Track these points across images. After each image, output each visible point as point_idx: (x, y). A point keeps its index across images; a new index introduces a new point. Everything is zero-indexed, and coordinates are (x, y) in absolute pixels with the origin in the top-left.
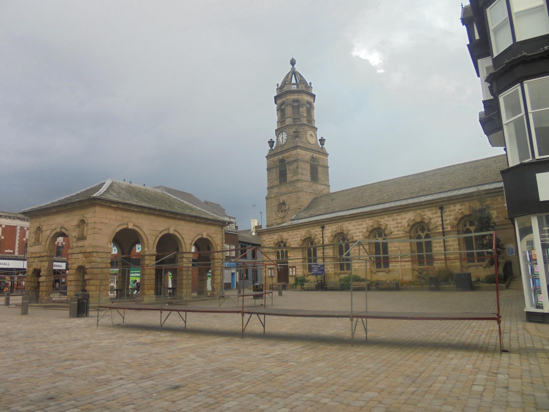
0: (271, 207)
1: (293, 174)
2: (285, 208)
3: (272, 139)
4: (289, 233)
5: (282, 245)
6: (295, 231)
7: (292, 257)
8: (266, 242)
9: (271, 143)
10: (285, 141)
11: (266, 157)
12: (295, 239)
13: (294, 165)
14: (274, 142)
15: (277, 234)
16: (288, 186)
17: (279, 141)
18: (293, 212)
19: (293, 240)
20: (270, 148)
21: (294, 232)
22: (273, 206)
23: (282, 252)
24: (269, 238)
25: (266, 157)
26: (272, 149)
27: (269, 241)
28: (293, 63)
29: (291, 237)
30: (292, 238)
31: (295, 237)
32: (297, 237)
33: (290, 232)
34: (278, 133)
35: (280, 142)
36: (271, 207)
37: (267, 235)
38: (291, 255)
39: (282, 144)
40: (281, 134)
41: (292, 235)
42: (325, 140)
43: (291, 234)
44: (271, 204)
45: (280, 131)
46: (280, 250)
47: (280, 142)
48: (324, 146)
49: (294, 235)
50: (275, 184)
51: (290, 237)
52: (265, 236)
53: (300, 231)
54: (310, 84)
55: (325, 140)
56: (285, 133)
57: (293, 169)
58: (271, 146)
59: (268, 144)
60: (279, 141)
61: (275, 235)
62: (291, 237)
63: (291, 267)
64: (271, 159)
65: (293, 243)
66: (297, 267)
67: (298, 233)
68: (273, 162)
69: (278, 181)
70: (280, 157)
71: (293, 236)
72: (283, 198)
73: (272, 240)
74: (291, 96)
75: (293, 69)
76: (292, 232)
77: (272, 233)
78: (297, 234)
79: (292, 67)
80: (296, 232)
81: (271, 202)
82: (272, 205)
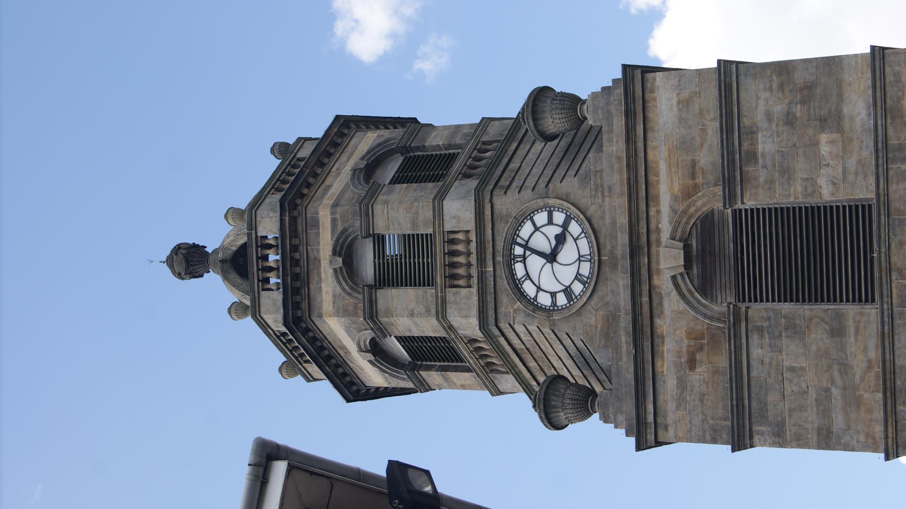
1: (823, 123)
11: (639, 448)
13: (760, 117)
17: (562, 300)
25: (639, 448)
34: (509, 306)
35: (568, 291)
39: (585, 269)
45: (502, 272)
47: (568, 291)
50: (874, 354)
56: (526, 230)
57: (790, 121)
64: (671, 412)
68: (692, 363)
69: (851, 310)
74: (330, 187)
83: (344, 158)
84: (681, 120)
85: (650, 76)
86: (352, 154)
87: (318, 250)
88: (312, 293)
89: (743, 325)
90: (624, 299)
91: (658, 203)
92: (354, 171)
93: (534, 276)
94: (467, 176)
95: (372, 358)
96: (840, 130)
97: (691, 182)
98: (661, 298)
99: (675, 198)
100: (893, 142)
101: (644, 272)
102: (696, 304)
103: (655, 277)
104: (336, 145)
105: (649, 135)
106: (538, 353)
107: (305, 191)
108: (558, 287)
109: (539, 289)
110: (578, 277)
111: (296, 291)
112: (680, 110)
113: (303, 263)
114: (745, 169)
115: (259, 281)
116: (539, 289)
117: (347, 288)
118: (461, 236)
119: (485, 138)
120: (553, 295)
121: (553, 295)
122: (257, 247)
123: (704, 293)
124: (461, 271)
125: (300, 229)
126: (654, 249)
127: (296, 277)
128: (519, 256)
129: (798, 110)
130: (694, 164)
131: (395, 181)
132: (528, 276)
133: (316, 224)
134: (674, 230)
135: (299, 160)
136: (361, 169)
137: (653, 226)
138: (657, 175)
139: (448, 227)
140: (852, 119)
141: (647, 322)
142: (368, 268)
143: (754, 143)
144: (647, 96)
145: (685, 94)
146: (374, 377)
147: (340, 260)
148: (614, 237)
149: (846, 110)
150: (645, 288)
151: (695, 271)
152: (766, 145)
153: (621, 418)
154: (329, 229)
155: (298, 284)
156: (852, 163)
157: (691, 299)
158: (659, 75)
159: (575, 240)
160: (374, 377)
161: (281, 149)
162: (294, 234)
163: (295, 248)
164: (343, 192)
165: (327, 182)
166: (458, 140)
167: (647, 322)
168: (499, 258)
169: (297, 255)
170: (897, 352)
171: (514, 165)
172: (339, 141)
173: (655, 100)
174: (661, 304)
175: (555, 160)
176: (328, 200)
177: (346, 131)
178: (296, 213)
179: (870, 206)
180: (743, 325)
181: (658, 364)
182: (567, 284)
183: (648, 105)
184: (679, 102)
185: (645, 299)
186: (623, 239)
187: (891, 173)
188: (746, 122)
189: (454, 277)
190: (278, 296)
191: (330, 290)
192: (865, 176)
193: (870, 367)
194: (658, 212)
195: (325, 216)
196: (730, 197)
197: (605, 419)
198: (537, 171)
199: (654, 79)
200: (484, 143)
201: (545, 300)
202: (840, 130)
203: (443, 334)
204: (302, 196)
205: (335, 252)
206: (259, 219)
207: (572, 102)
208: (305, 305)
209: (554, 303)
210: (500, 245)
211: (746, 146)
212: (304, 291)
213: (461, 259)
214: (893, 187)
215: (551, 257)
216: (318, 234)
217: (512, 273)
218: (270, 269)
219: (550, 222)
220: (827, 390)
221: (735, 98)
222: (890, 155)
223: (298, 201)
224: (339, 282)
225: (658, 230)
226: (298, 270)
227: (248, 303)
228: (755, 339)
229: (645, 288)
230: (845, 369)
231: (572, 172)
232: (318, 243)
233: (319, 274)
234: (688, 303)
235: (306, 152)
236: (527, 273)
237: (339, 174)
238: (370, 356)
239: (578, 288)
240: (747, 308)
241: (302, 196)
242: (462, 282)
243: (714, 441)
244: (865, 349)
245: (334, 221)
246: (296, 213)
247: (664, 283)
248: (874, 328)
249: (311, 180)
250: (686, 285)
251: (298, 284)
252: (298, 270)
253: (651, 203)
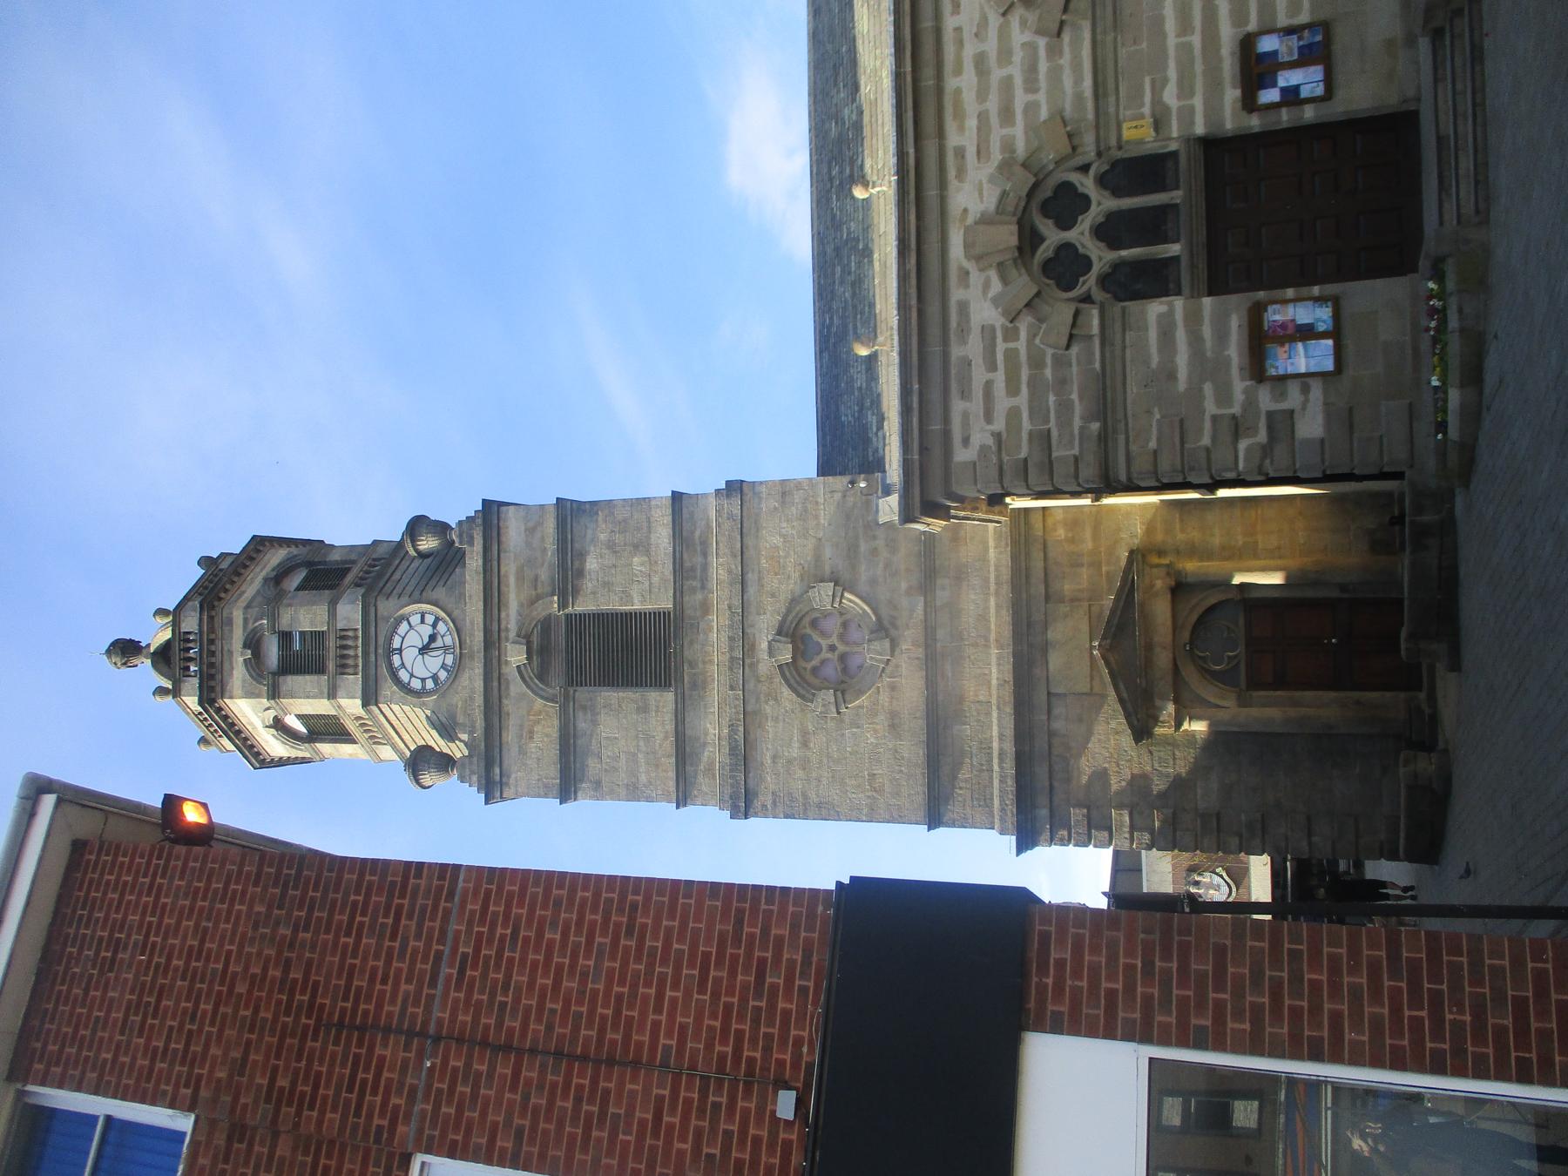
0: (805, 764)
2: (834, 640)
4: (960, 153)
5: (1053, 236)
6: (951, 83)
7: (1157, 89)
8: (1014, 414)
12: (1018, 81)
15: (956, 294)
16: (699, 596)
17: (430, 684)
18: (863, 547)
19: (1020, 99)
21: (958, 91)
22: (805, 744)
23: (1108, 232)
24: (988, 386)
27: (1013, 390)
29: (994, 120)
30: (1007, 115)
31: (997, 74)
32: (1005, 55)
33: (953, 139)
35: (435, 678)
36: (805, 764)
37: (958, 406)
38: (1147, 110)
40: (396, 660)
41: (983, 118)
43: (972, 123)
44: (790, 762)
46: (1101, 257)
47: (435, 678)
49: (982, 95)
50: (670, 727)
51: (997, 135)
52: (966, 441)
53: (958, 30)
57: (611, 546)
58: (445, 763)
61: (964, 307)
62: (994, 120)
63: (1249, 103)
65: (1041, 97)
66: (1252, 26)
67: (969, 51)
69: (653, 696)
70: (515, 656)
71: (993, 105)
72: (764, 627)
73: (1001, 347)
74: (244, 592)
76: (959, 115)
77: (945, 342)
78: (980, 61)
80: (962, 83)
81: (775, 758)
82: (795, 751)
83: (257, 570)
84: (528, 544)
85: (503, 509)
86: (265, 567)
87: (231, 644)
88: (225, 680)
89: (571, 704)
90: (479, 684)
91: (507, 607)
92: (266, 580)
93: (409, 666)
94: (358, 585)
95: (275, 733)
96: (647, 553)
97: (534, 593)
98: (508, 683)
99: (521, 605)
100: (687, 564)
101: (495, 662)
102: (534, 686)
103: (503, 667)
104: (252, 559)
105: (502, 555)
106: (410, 727)
107: (223, 595)
109: (412, 675)
110: (444, 666)
111: (212, 677)
112: (526, 536)
113: (218, 654)
114: (575, 582)
115: (180, 669)
116: (412, 675)
117: (254, 674)
118: (350, 634)
119: (374, 556)
120: (423, 680)
121: (423, 680)
122: (180, 640)
123: (541, 678)
124: (350, 662)
125: (216, 626)
126: (503, 645)
127: (212, 665)
128: (397, 649)
129: (618, 538)
130: (536, 579)
131: (298, 589)
133: (230, 622)
134: (520, 630)
135: (221, 570)
136: (272, 579)
137: (503, 626)
138: (508, 586)
139: (340, 626)
140: (657, 546)
141: (496, 701)
143: (583, 562)
144: (501, 524)
145: (531, 524)
146: (274, 746)
147: (249, 651)
148: (472, 635)
149: (653, 541)
150: (496, 675)
151: (535, 663)
152: (592, 564)
153: (475, 778)
154: (241, 626)
155: (213, 671)
156: (656, 579)
157: (531, 684)
158: (512, 508)
159: (442, 637)
160: (274, 746)
161: (205, 562)
162: (212, 630)
163: (211, 642)
164: (254, 598)
165: (243, 588)
166: (353, 557)
167: (496, 701)
168: (380, 651)
169: (213, 648)
170: (686, 726)
171: (397, 576)
172: (255, 556)
173: (507, 528)
174: (508, 688)
175: (429, 574)
176: (242, 603)
177: (261, 548)
178: (213, 613)
179: (669, 613)
180: (571, 704)
181: (504, 735)
183: (502, 531)
184: (526, 530)
185: (495, 684)
186: (479, 636)
187: (685, 587)
188: (577, 546)
189: (344, 666)
190: (195, 681)
191: (241, 676)
192: (666, 590)
193: (666, 738)
194: (508, 615)
195: (238, 616)
196: (563, 605)
197: (462, 779)
198: (413, 582)
199: (508, 511)
200: (374, 560)
201: (416, 684)
202: (647, 553)
203: (333, 712)
204: (220, 599)
205: (246, 646)
206: (182, 618)
207: (441, 528)
208: (218, 689)
209: (424, 687)
210: (381, 640)
211: (577, 564)
212: (218, 677)
213: (351, 652)
214: (686, 599)
216: (231, 631)
217: (390, 664)
218: (191, 659)
219: (423, 621)
220: (634, 755)
221: (569, 526)
222: (685, 574)
223: (216, 603)
224: (248, 670)
225: (507, 630)
226: (213, 660)
227: (171, 687)
228: (580, 715)
229: (496, 675)
230: (648, 738)
231: (442, 583)
232: (232, 638)
233: (231, 663)
234: (528, 686)
235: (224, 565)
236: (403, 664)
237: (252, 583)
238: (273, 731)
239: (443, 675)
240: (575, 691)
241: (220, 599)
242: (350, 670)
243: (546, 796)
244: (663, 724)
245: (246, 620)
246: (213, 613)
247: (510, 671)
248: (671, 706)
249: (228, 586)
250: (528, 673)
251: (213, 671)
252: (213, 660)
253: (502, 609)
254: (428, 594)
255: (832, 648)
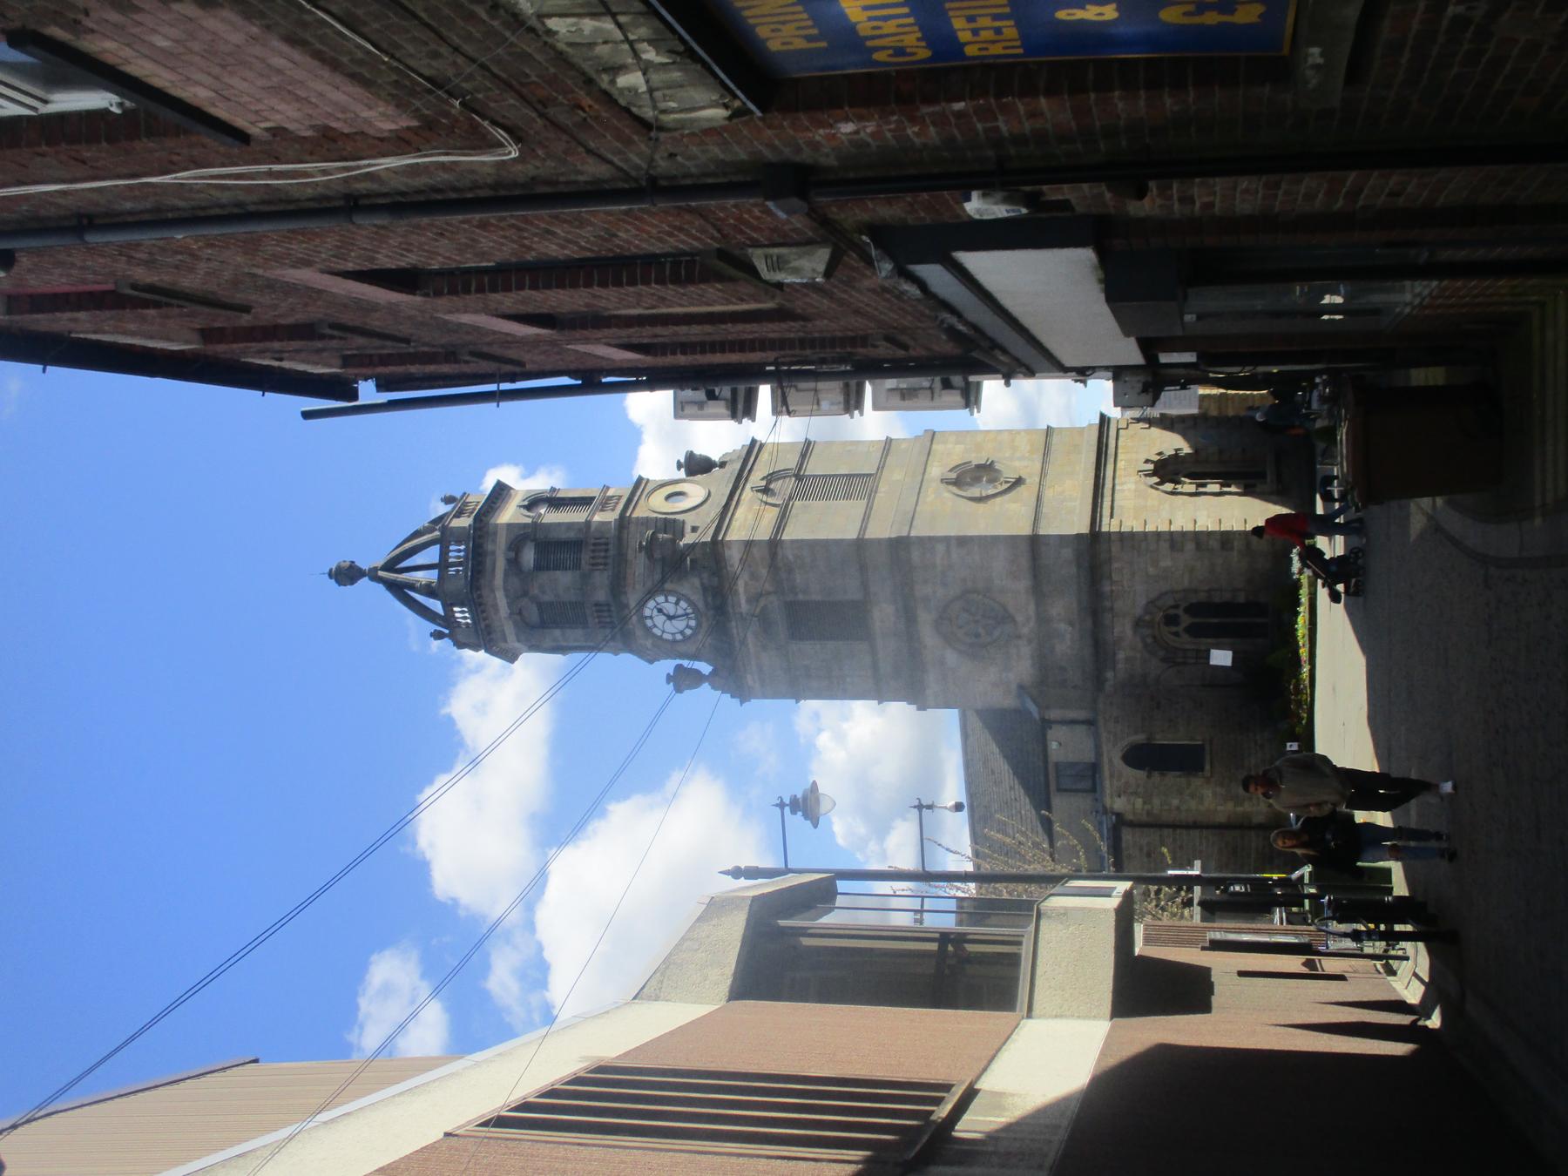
3: (668, 675)
9: (683, 680)
10: (683, 604)
14: (679, 668)
17: (679, 637)
20: (706, 686)
25: (741, 705)
26: (714, 673)
28: (347, 575)
35: (682, 632)
39: (693, 623)
40: (649, 623)
42: (691, 457)
48: (716, 457)
54: (448, 500)
55: (691, 457)
56: (651, 604)
58: (695, 679)
59: (687, 692)
60: (679, 637)
75: (373, 575)
79: (366, 579)
93: (660, 626)
108: (674, 631)
109: (663, 632)
110: (688, 626)
120: (672, 634)
132: (655, 626)
142: (533, 614)
182: (681, 629)
197: (714, 687)
201: (666, 636)
213: (606, 614)
215: (670, 618)
217: (645, 626)
219: (667, 601)
254: (668, 586)
255: (977, 622)
